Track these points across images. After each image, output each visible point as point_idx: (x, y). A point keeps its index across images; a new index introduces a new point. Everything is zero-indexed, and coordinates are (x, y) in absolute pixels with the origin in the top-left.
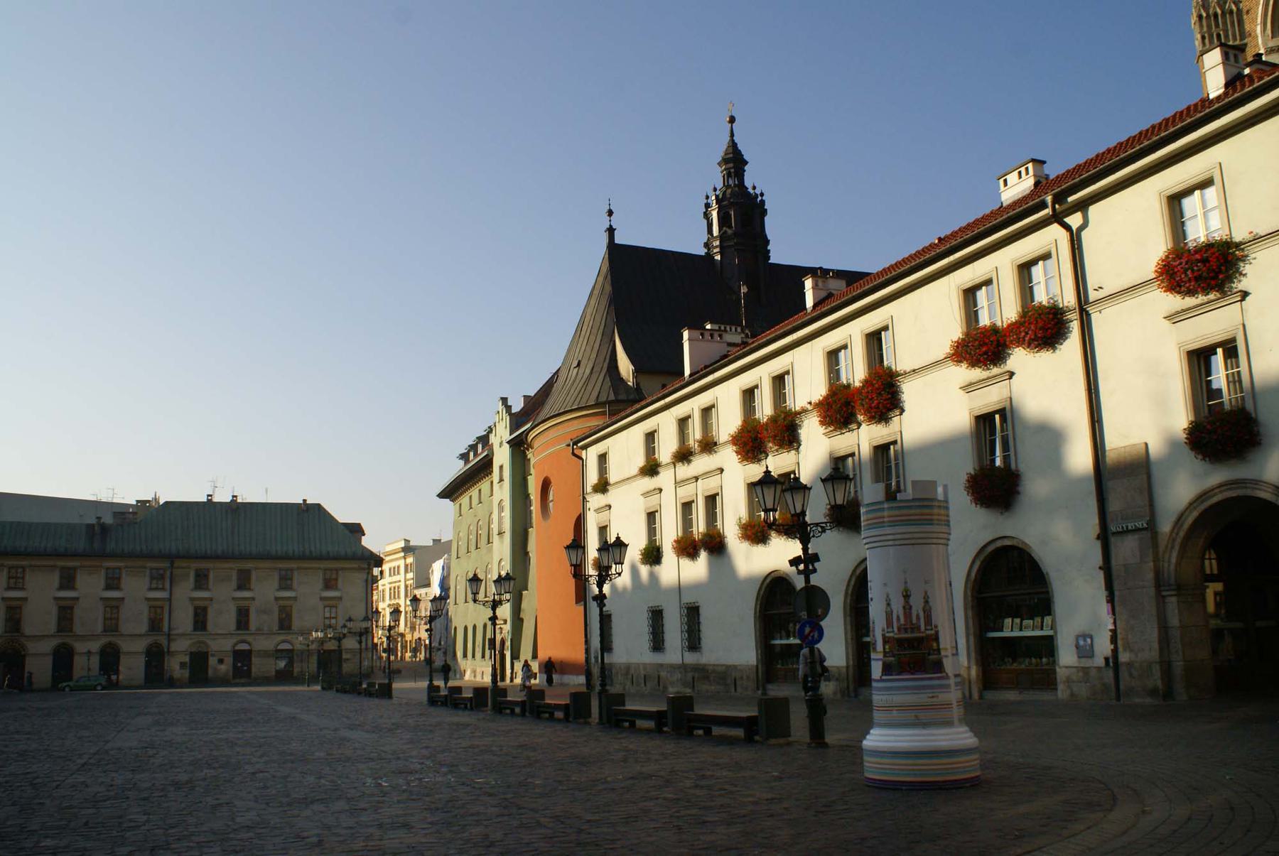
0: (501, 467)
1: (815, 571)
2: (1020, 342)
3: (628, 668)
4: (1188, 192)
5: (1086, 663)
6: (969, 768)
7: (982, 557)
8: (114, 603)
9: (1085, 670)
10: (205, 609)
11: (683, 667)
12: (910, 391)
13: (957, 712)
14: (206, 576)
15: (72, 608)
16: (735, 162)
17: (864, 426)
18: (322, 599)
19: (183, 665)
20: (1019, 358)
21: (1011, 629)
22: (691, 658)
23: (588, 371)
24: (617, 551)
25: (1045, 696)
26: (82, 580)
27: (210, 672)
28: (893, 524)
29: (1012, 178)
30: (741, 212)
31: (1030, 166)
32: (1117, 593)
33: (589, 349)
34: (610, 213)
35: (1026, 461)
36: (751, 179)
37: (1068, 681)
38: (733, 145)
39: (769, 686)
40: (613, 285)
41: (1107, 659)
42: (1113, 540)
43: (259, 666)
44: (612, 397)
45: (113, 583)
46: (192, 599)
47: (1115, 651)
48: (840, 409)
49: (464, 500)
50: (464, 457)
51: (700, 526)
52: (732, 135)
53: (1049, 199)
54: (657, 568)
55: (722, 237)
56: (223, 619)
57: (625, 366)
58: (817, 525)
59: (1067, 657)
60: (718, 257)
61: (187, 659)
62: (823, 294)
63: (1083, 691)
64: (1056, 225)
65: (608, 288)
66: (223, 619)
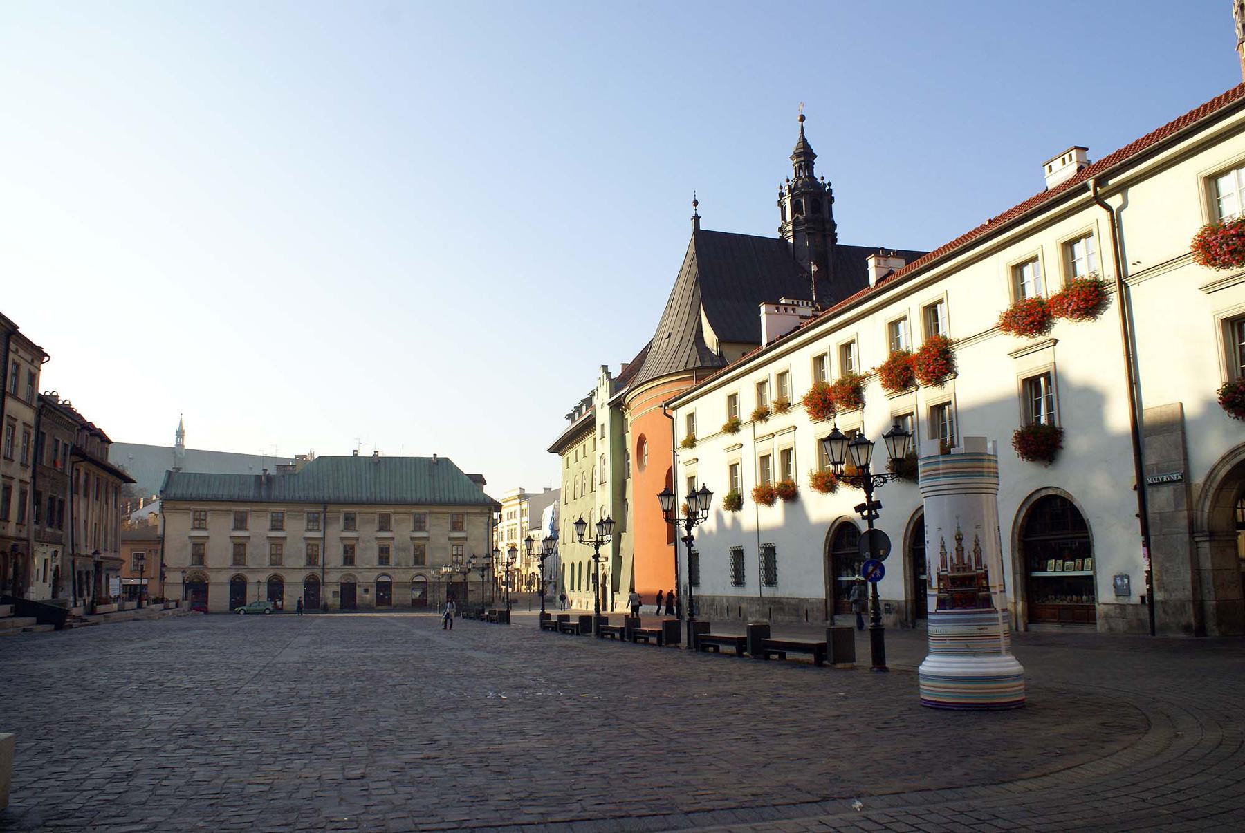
1: (877, 516)
2: (1063, 313)
3: (713, 599)
6: (1015, 692)
7: (1028, 506)
8: (278, 542)
9: (1122, 607)
10: (353, 547)
11: (761, 600)
12: (961, 358)
13: (1003, 642)
14: (354, 519)
15: (244, 545)
16: (805, 156)
17: (921, 388)
18: (450, 539)
19: (335, 593)
20: (1063, 327)
21: (1053, 569)
22: (768, 592)
23: (677, 342)
24: (703, 499)
25: (1086, 630)
26: (251, 521)
27: (358, 601)
28: (946, 475)
29: (1057, 164)
30: (811, 201)
31: (1074, 153)
32: (1152, 539)
33: (678, 322)
34: (696, 203)
35: (1069, 420)
37: (1107, 616)
38: (804, 141)
39: (836, 617)
41: (1143, 598)
42: (1149, 490)
43: (398, 595)
44: (699, 364)
45: (277, 525)
46: (342, 539)
47: (1150, 591)
48: (900, 374)
49: (571, 454)
50: (571, 417)
51: (776, 478)
52: (803, 132)
53: (1091, 183)
54: (738, 513)
55: (794, 223)
56: (367, 555)
57: (710, 337)
58: (879, 476)
59: (1105, 595)
60: (791, 241)
61: (338, 589)
62: (885, 272)
63: (1120, 625)
64: (1097, 206)
65: (695, 269)
66: (367, 555)
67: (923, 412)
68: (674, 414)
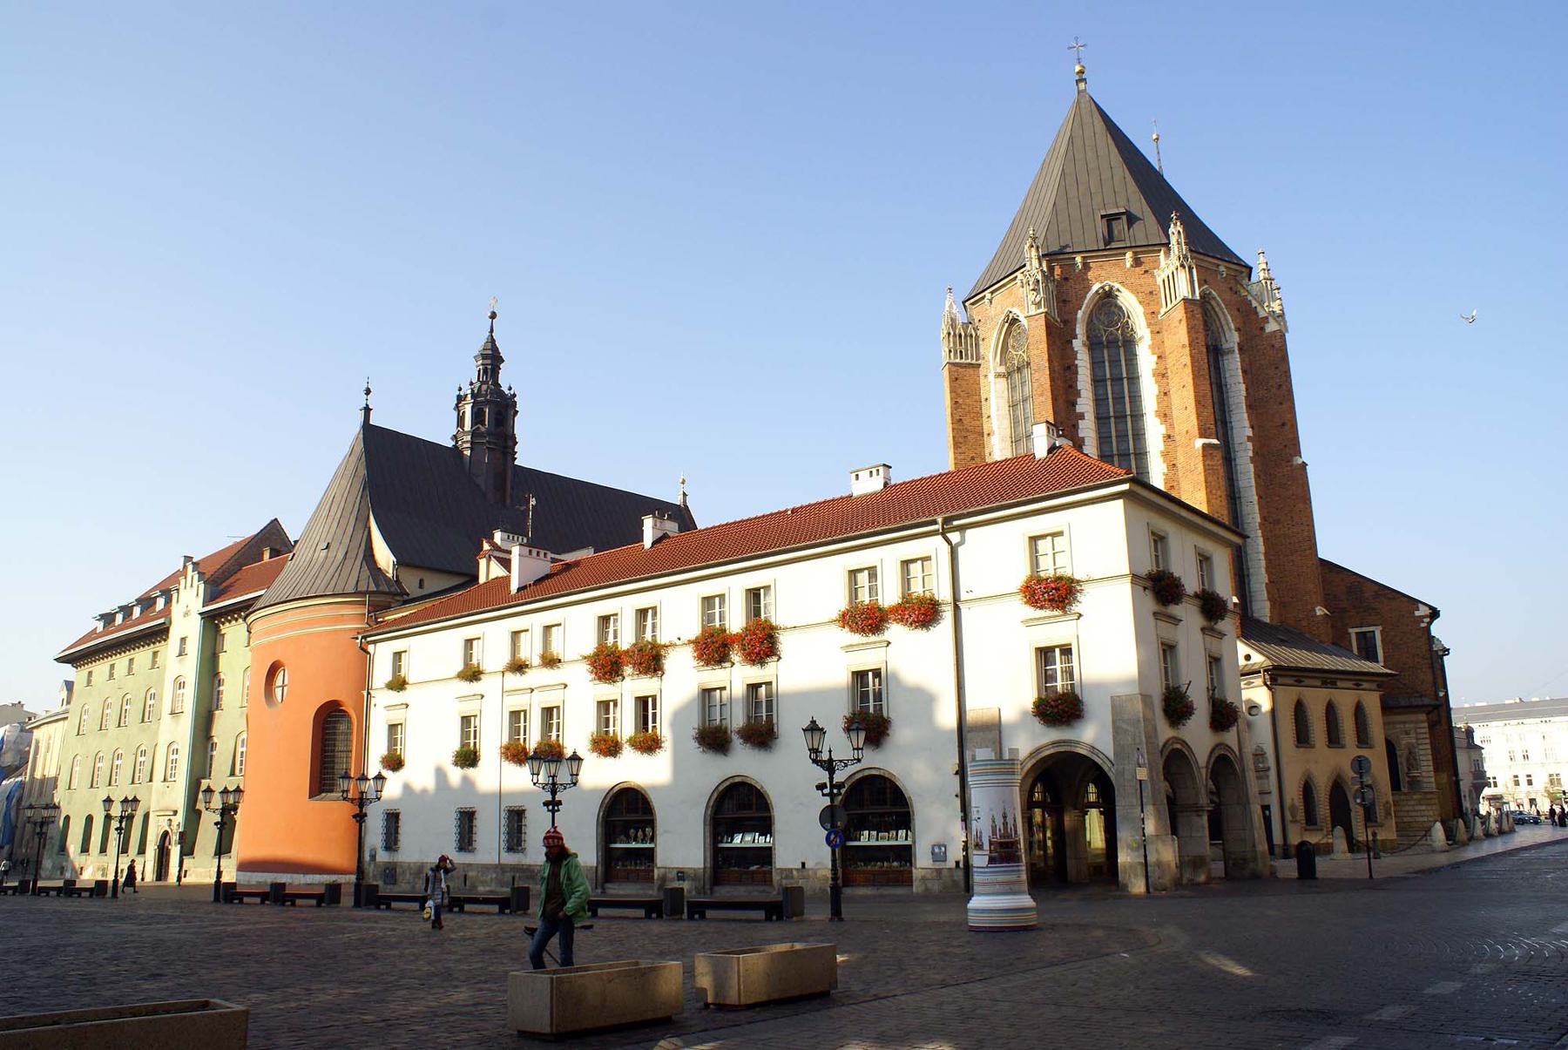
0: (183, 640)
2: (901, 620)
4: (1043, 537)
5: (939, 865)
6: (1031, 919)
9: (939, 871)
11: (501, 868)
12: (785, 642)
13: (1025, 887)
16: (492, 359)
17: (737, 665)
20: (896, 631)
21: (867, 839)
22: (510, 859)
23: (340, 556)
24: (575, 764)
25: (899, 891)
28: (994, 774)
33: (340, 532)
34: (368, 392)
35: (895, 709)
36: (505, 380)
37: (923, 879)
38: (493, 341)
40: (368, 466)
41: (957, 863)
44: (373, 588)
47: (966, 858)
48: (713, 648)
50: (108, 618)
51: (533, 740)
53: (940, 520)
54: (471, 771)
55: (474, 434)
59: (923, 860)
60: (468, 453)
63: (936, 887)
64: (940, 537)
65: (363, 471)
67: (739, 690)
68: (371, 648)
